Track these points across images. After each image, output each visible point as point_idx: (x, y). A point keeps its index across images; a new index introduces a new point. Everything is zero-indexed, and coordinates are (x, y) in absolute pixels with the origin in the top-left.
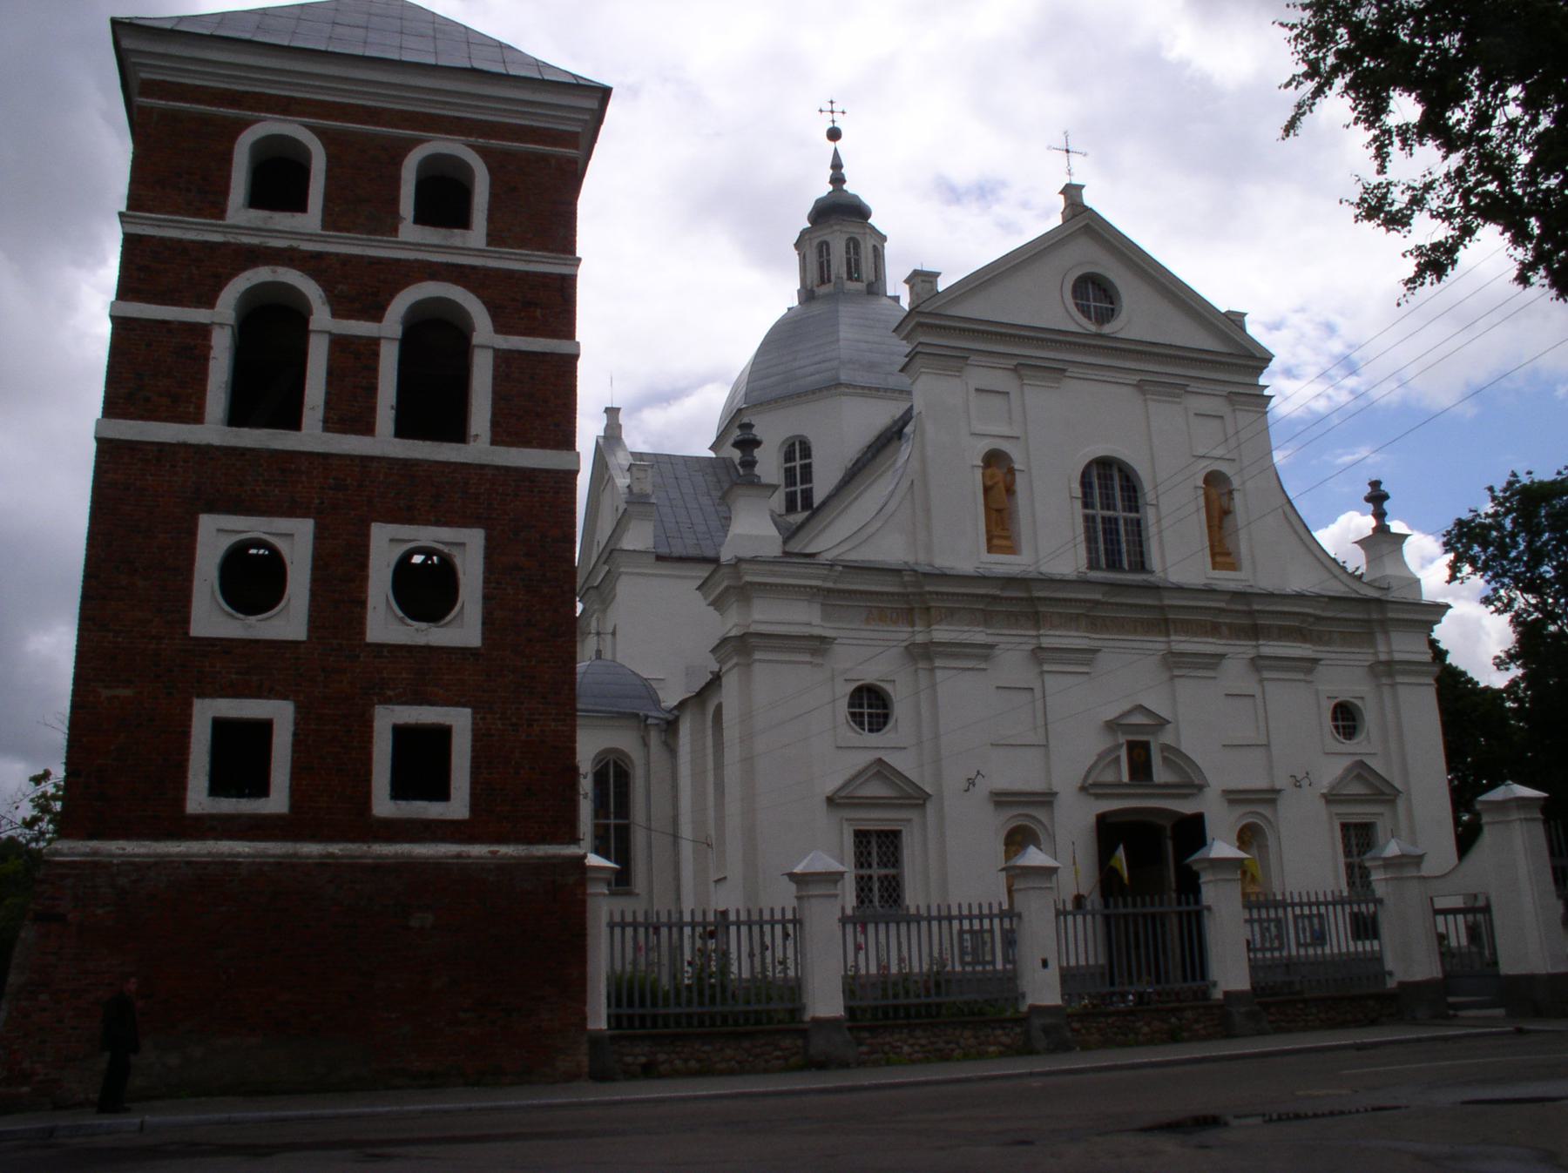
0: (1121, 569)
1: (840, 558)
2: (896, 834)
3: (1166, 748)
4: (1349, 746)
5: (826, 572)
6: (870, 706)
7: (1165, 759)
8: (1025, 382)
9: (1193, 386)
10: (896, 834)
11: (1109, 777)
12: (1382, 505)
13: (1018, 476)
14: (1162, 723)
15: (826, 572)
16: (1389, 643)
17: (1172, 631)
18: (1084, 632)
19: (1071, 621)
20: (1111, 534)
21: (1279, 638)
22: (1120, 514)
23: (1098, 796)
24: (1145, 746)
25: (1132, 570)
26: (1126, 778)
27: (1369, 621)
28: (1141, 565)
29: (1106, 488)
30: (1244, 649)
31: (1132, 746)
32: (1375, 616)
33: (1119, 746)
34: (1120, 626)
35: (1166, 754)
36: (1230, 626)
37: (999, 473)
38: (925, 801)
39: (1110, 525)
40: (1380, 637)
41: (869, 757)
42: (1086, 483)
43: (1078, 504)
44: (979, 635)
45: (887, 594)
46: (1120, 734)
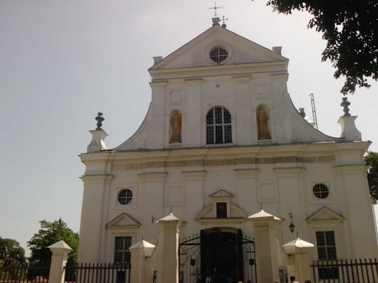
0: (222, 143)
11: (209, 215)
14: (231, 196)
21: (286, 162)
22: (223, 125)
23: (202, 223)
24: (225, 204)
25: (226, 142)
26: (215, 215)
29: (218, 116)
31: (218, 204)
33: (212, 204)
36: (265, 159)
38: (139, 227)
39: (219, 129)
42: (209, 116)
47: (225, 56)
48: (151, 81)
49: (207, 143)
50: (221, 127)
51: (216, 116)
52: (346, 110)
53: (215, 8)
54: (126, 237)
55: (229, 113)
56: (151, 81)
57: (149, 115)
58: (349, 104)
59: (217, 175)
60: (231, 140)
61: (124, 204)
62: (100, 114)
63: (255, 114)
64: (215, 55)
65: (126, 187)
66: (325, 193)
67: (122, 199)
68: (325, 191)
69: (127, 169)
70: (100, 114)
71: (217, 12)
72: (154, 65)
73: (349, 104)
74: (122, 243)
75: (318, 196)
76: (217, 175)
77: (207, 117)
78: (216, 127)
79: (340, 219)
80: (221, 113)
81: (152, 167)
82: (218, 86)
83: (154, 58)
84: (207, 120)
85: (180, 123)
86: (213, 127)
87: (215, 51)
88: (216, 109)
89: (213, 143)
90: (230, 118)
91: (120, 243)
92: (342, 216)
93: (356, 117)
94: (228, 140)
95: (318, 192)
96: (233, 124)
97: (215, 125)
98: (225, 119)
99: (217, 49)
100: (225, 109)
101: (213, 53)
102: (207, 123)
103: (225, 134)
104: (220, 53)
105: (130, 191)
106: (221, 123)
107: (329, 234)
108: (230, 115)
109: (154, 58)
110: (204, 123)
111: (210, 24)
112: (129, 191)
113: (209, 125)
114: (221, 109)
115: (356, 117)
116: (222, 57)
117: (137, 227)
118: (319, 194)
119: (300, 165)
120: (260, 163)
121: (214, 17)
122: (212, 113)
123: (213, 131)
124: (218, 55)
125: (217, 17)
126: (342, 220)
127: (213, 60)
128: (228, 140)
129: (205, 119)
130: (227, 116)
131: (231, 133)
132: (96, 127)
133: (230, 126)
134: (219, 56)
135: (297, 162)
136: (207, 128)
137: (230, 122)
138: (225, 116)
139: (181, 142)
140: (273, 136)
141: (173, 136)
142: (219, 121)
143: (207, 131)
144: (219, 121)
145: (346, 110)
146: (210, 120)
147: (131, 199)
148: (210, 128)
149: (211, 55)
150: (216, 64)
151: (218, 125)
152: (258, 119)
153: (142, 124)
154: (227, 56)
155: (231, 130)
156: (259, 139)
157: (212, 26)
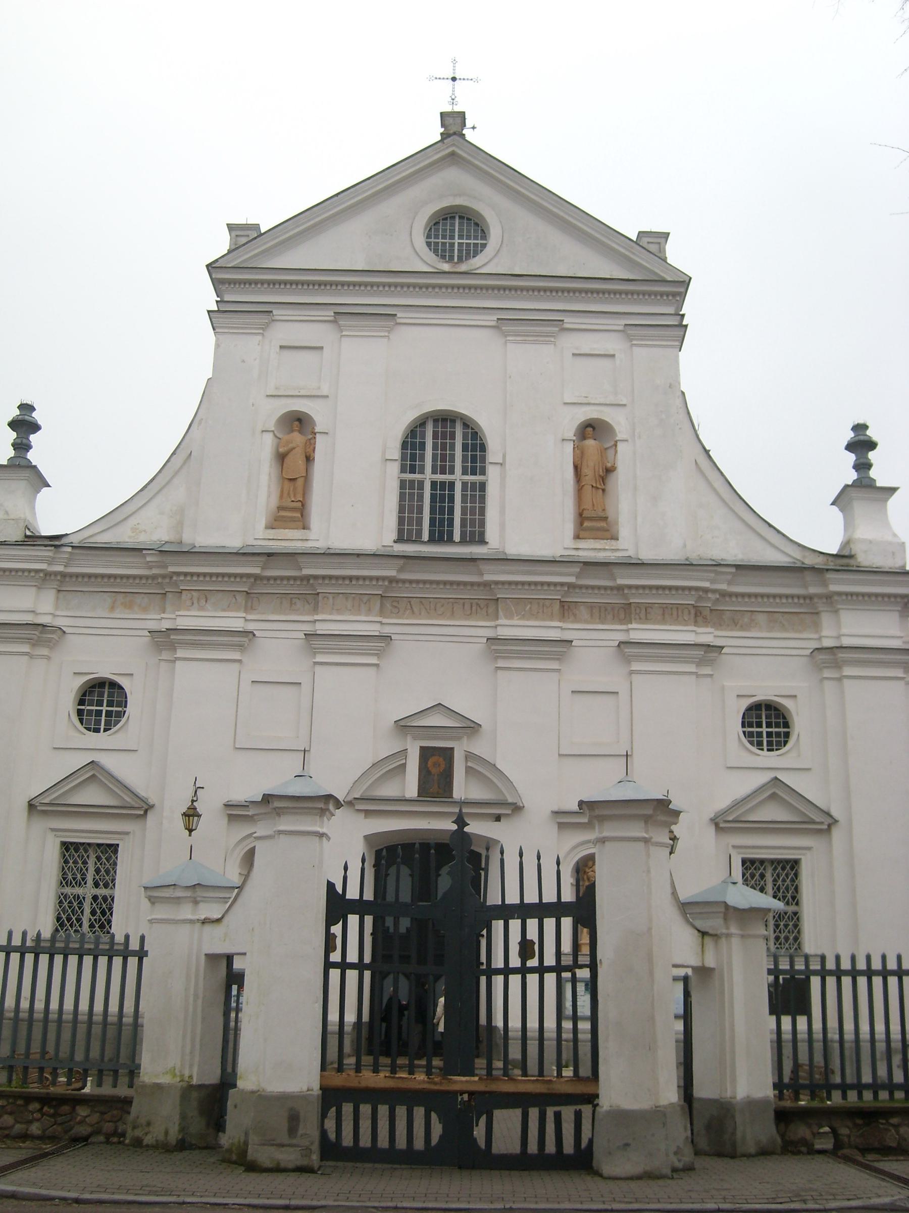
0: (450, 540)
1: (91, 540)
2: (114, 848)
3: (469, 756)
4: (767, 758)
5: (50, 554)
6: (100, 703)
7: (469, 770)
8: (344, 333)
9: (570, 321)
10: (114, 848)
11: (389, 790)
12: (867, 453)
13: (320, 440)
14: (471, 728)
15: (50, 554)
16: (838, 625)
17: (501, 613)
18: (376, 616)
19: (360, 602)
20: (442, 500)
21: (663, 621)
22: (458, 477)
23: (368, 813)
24: (448, 754)
25: (463, 541)
26: (412, 790)
27: (811, 597)
29: (444, 448)
31: (425, 753)
32: (812, 590)
34: (431, 607)
35: (469, 764)
36: (591, 607)
37: (298, 439)
38: (146, 811)
40: (826, 619)
41: (84, 759)
43: (395, 468)
44: (234, 621)
45: (134, 577)
46: (409, 738)
47: (476, 245)
48: (214, 307)
49: (400, 540)
50: (452, 485)
51: (435, 448)
52: (863, 466)
53: (454, 79)
54: (99, 845)
55: (481, 440)
56: (214, 307)
57: (200, 423)
58: (871, 445)
60: (482, 534)
61: (97, 730)
62: (26, 408)
63: (569, 448)
64: (444, 237)
65: (105, 673)
66: (778, 734)
67: (90, 712)
68: (777, 725)
69: (112, 608)
70: (26, 408)
71: (456, 94)
72: (230, 252)
73: (872, 445)
74: (85, 863)
75: (755, 739)
77: (404, 446)
78: (434, 484)
79: (822, 823)
80: (453, 436)
81: (202, 608)
83: (231, 227)
84: (403, 458)
85: (309, 459)
86: (421, 484)
88: (436, 421)
89: (418, 540)
90: (483, 459)
91: (75, 862)
92: (828, 814)
93: (892, 490)
94: (472, 533)
95: (755, 730)
96: (493, 476)
97: (428, 476)
98: (465, 459)
100: (466, 425)
101: (437, 230)
102: (403, 470)
103: (464, 511)
105: (121, 688)
106: (452, 472)
107: (783, 869)
108: (483, 448)
109: (231, 227)
110: (394, 469)
111: (434, 133)
112: (114, 685)
113: (409, 476)
115: (892, 490)
116: (468, 245)
117: (142, 812)
119: (706, 635)
120: (576, 620)
121: (448, 108)
122: (423, 436)
123: (421, 497)
124: (452, 237)
125: (457, 109)
126: (829, 826)
127: (436, 252)
128: (472, 533)
129: (396, 454)
130: (474, 449)
131: (482, 511)
132: (11, 453)
133: (483, 486)
134: (457, 241)
135: (696, 623)
136: (403, 485)
137: (483, 472)
138: (465, 448)
139: (305, 527)
140: (624, 532)
141: (280, 508)
142: (443, 464)
143: (402, 497)
144: (443, 464)
145: (863, 466)
146: (413, 458)
147: (120, 715)
148: (412, 487)
149: (429, 236)
150: (446, 267)
151: (440, 477)
152: (577, 469)
153: (174, 453)
154: (484, 246)
155: (483, 499)
156: (577, 537)
157: (439, 138)
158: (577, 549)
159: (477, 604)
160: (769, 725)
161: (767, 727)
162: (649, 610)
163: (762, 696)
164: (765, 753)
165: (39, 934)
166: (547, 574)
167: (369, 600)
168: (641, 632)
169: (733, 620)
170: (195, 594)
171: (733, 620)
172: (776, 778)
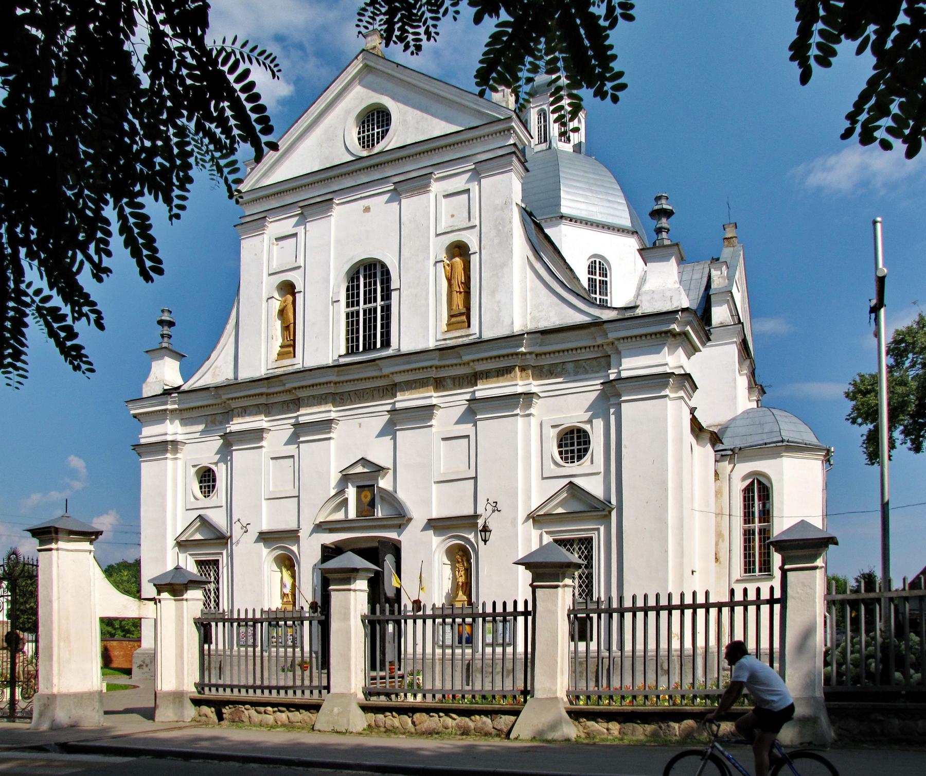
1: (195, 386)
28: (386, 343)
30: (459, 398)
51: (365, 286)
59: (360, 425)
76: (360, 425)
82: (367, 209)
87: (368, 121)
99: (373, 115)
104: (378, 122)
114: (375, 265)
118: (579, 450)
134: (376, 130)
149: (359, 133)
158: (445, 340)
159: (387, 389)
160: (572, 444)
161: (574, 446)
162: (488, 374)
163: (568, 424)
164: (570, 465)
165: (434, 605)
166: (415, 362)
167: (326, 397)
168: (486, 389)
169: (550, 371)
170: (239, 409)
171: (550, 371)
172: (571, 482)
